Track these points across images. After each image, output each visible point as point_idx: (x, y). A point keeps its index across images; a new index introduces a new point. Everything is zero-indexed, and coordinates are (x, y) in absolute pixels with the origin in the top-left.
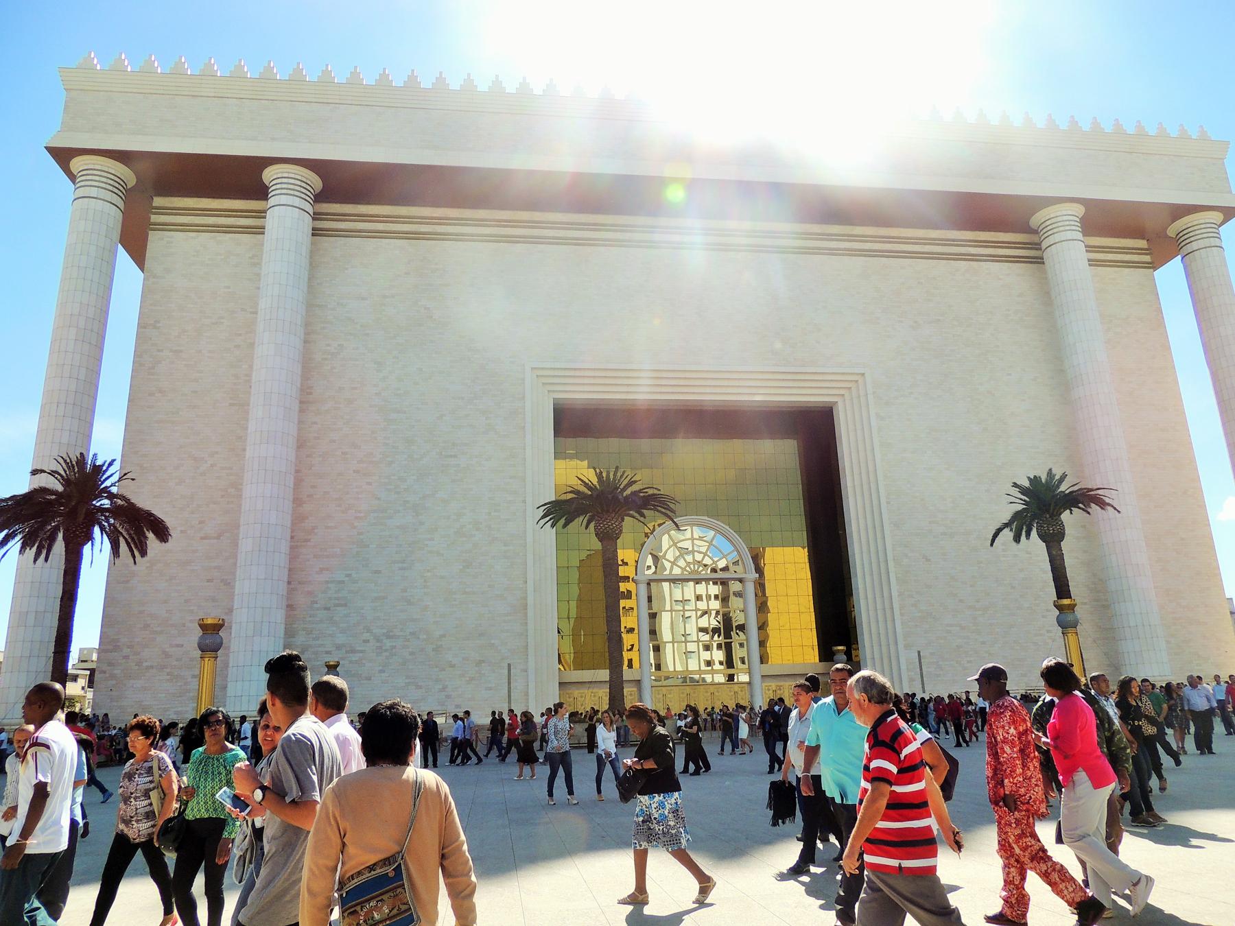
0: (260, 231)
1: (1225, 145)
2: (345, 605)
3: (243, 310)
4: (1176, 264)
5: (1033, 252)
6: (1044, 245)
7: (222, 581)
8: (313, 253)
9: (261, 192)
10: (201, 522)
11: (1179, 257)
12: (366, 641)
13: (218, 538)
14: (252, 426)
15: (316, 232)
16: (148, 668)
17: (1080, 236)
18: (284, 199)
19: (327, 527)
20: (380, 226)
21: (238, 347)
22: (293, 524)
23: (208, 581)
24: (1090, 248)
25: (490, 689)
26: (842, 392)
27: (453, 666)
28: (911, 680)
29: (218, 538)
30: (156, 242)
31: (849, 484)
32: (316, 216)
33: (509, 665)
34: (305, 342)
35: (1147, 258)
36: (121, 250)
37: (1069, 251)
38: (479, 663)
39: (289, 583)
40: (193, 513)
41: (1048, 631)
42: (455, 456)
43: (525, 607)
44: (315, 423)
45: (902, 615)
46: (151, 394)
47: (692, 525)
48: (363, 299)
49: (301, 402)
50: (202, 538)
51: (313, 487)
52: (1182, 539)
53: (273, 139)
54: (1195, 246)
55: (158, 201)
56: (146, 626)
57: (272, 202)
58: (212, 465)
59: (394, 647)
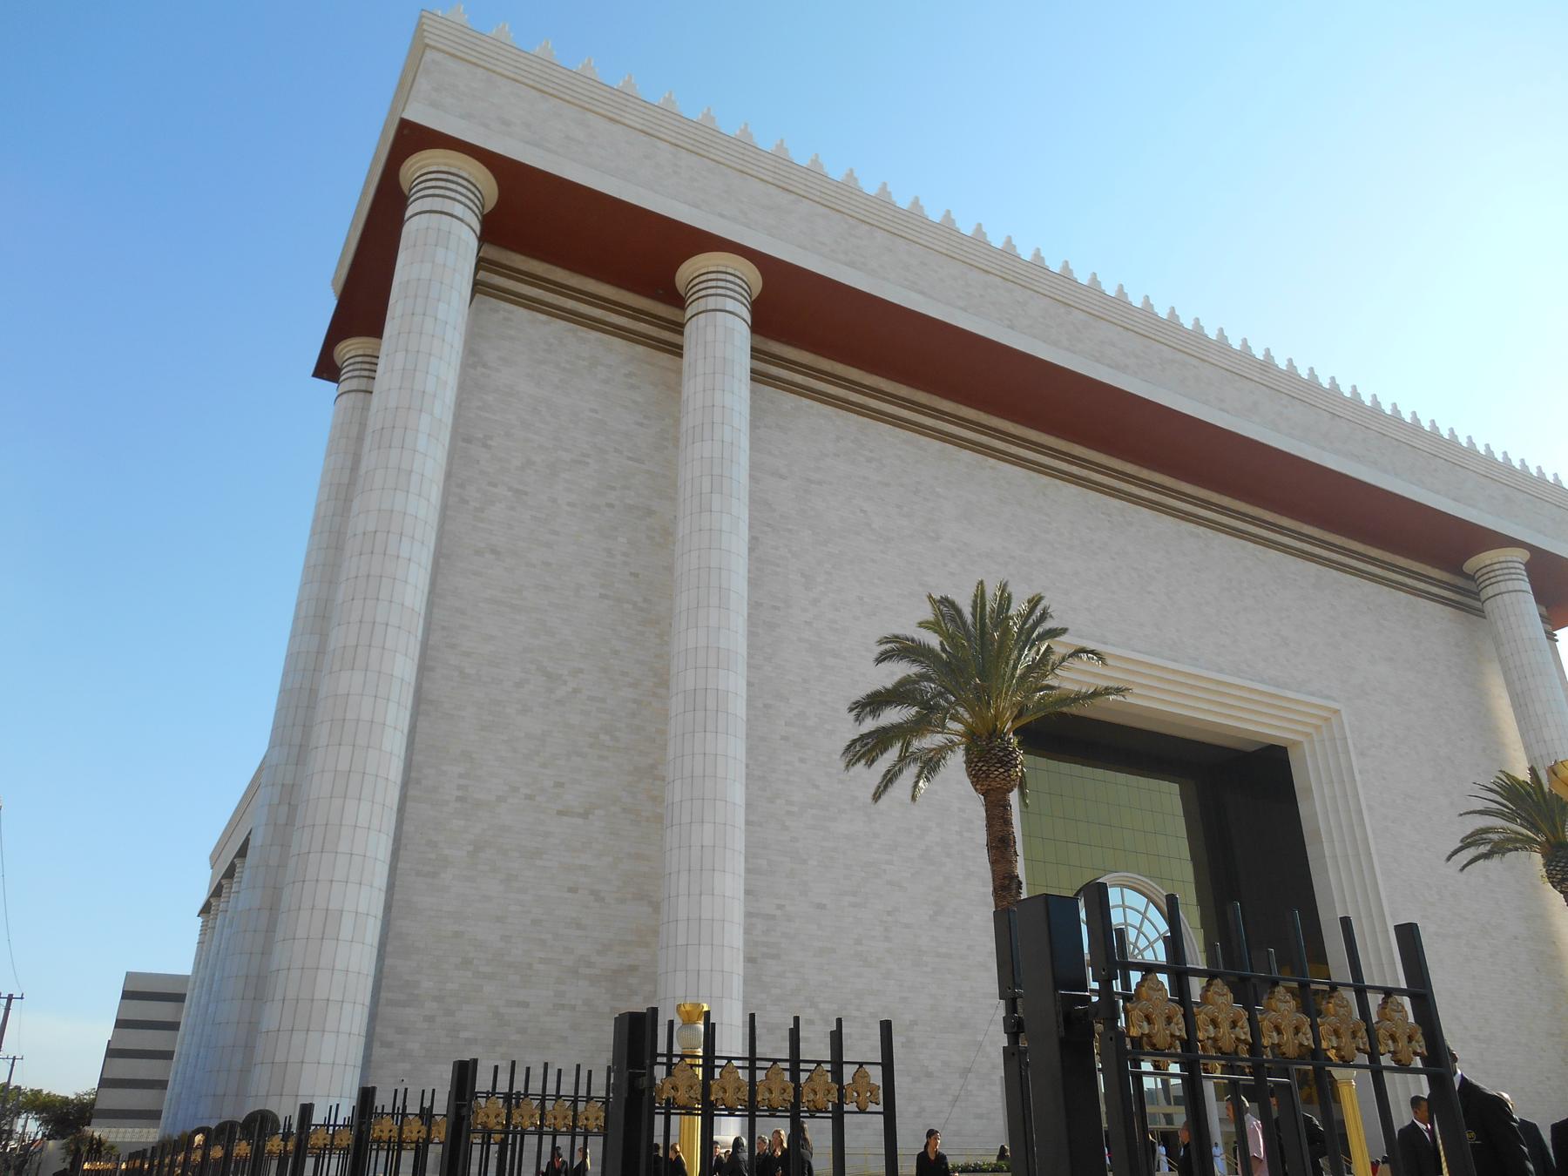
3: (616, 450)
5: (1468, 597)
10: (559, 785)
13: (585, 815)
20: (799, 378)
21: (610, 506)
23: (571, 890)
27: (929, 1075)
37: (1518, 603)
38: (965, 1072)
48: (782, 477)
50: (560, 813)
53: (722, 216)
58: (575, 691)
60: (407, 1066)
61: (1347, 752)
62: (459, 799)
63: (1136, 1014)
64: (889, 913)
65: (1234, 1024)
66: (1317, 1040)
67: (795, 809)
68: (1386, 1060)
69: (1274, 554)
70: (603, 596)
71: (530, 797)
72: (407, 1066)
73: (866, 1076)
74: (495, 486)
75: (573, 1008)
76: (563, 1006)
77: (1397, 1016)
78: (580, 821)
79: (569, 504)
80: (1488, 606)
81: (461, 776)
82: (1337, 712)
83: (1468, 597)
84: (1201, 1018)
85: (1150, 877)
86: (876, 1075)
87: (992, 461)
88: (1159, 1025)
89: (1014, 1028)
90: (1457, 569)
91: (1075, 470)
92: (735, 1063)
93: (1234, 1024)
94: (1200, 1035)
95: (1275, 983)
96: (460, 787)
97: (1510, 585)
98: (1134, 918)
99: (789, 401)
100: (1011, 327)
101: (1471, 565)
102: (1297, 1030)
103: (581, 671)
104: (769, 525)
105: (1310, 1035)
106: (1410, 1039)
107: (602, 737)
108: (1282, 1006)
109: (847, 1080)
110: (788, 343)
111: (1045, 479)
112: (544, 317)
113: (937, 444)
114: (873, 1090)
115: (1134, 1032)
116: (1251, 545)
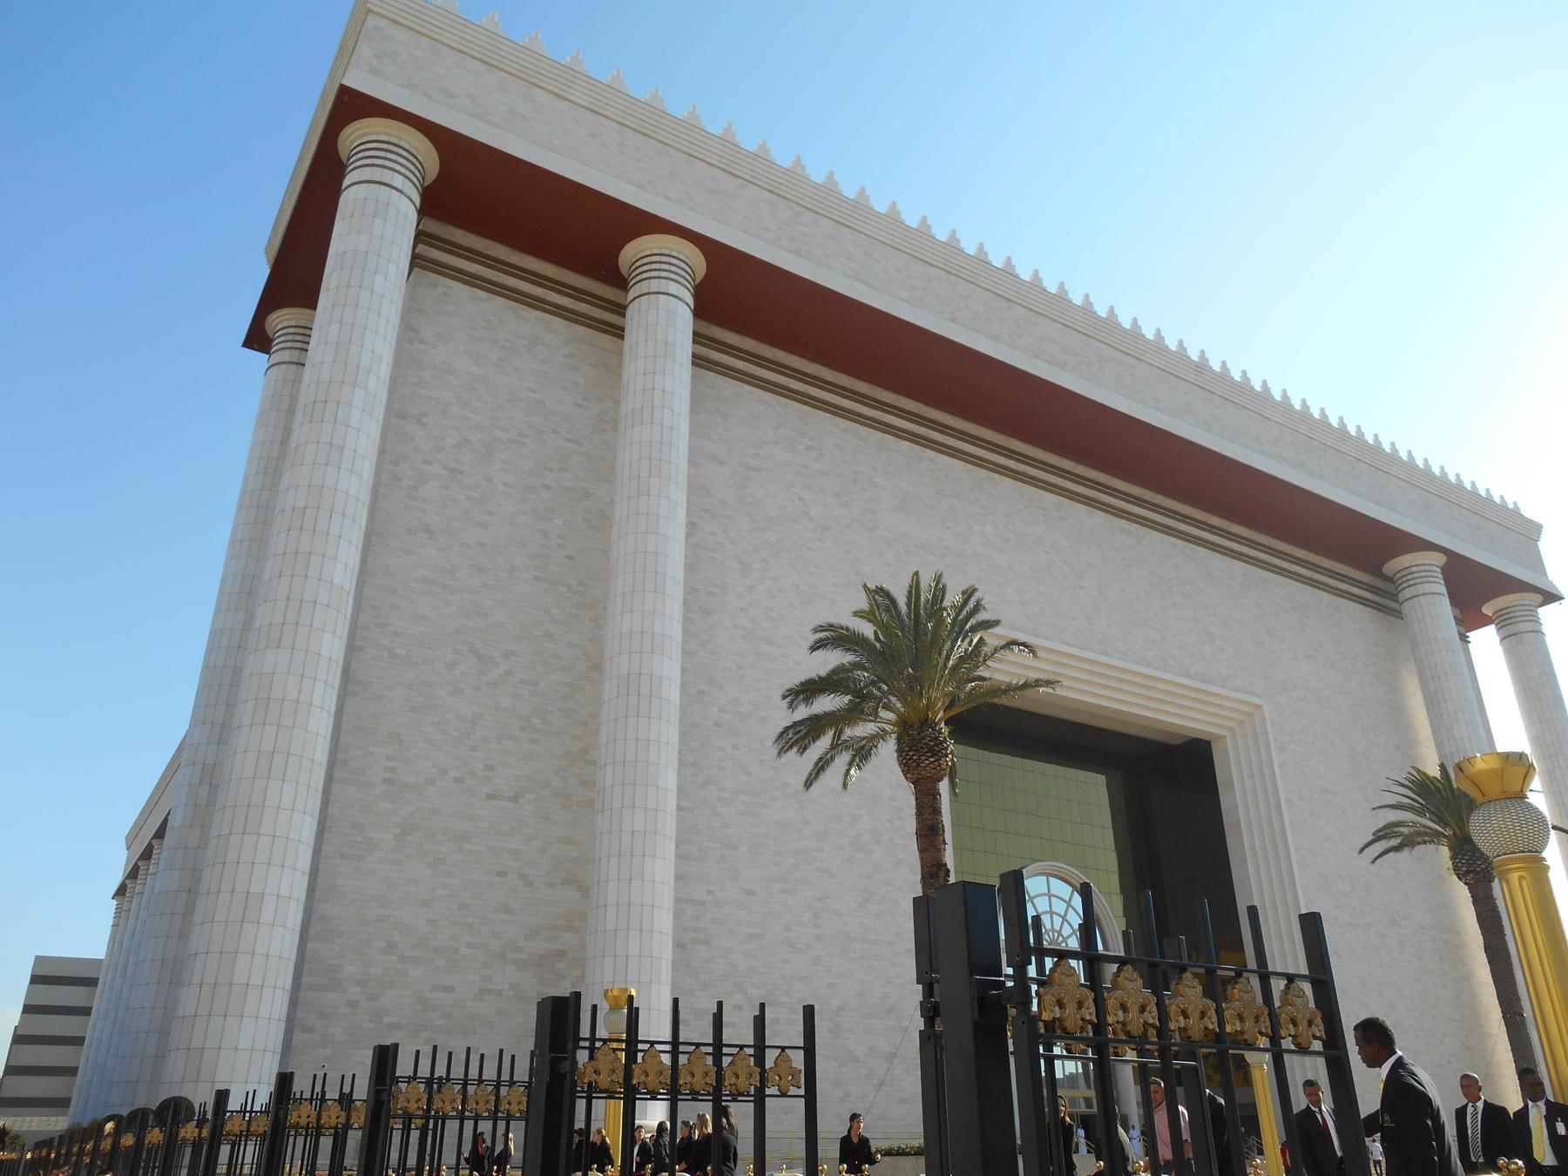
1: (1537, 528)
2: (706, 943)
3: (554, 431)
5: (1386, 598)
7: (522, 877)
13: (515, 799)
20: (740, 365)
23: (499, 874)
27: (855, 1060)
37: (1433, 605)
40: (474, 749)
46: (411, 532)
47: (1048, 875)
48: (721, 463)
50: (489, 797)
53: (666, 197)
56: (391, 947)
58: (507, 673)
60: (328, 1052)
61: (1269, 746)
62: (386, 781)
63: (1048, 999)
64: (818, 900)
65: (1143, 1009)
66: (1221, 1023)
67: (727, 795)
68: (1287, 1043)
69: (1202, 552)
70: (536, 578)
71: (457, 780)
72: (328, 1052)
73: (789, 1060)
74: (430, 464)
75: (500, 993)
76: (489, 991)
77: (1298, 1001)
78: (511, 805)
79: (505, 484)
80: (1406, 607)
81: (388, 758)
82: (1259, 707)
83: (1386, 598)
84: (1111, 1003)
85: (1076, 867)
86: (798, 1059)
87: (930, 453)
88: (1071, 1009)
89: (931, 1011)
90: (1376, 569)
92: (659, 1047)
93: (1143, 1009)
94: (1110, 1019)
95: (1183, 969)
96: (387, 769)
97: (1427, 588)
98: (1059, 907)
99: (730, 386)
100: (953, 320)
101: (1391, 567)
102: (1203, 1015)
103: (513, 653)
104: (707, 511)
105: (1215, 1019)
106: (1310, 1023)
107: (534, 720)
108: (1190, 992)
109: (769, 1064)
111: (983, 473)
113: (879, 435)
114: (795, 1073)
115: (1046, 1016)
116: (1181, 542)
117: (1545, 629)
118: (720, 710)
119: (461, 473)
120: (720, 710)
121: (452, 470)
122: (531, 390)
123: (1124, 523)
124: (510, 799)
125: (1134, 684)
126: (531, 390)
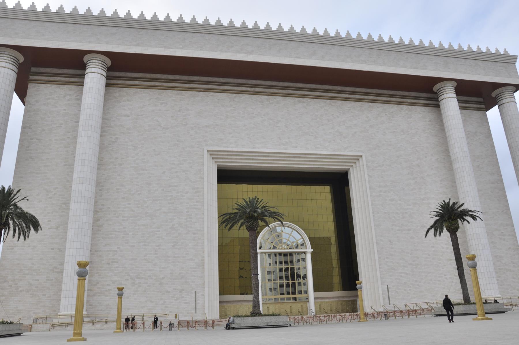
0: (82, 84)
3: (71, 120)
4: (496, 108)
6: (440, 99)
8: (106, 93)
9: (83, 67)
11: (497, 106)
12: (128, 280)
13: (57, 228)
14: (75, 176)
15: (108, 85)
16: (21, 291)
17: (455, 96)
18: (93, 70)
19: (109, 225)
20: (137, 83)
21: (68, 138)
22: (93, 223)
23: (52, 249)
24: (459, 101)
25: (186, 303)
26: (352, 164)
27: (169, 292)
28: (384, 299)
29: (57, 228)
30: (32, 89)
31: (355, 207)
32: (108, 78)
33: (196, 292)
34: (101, 136)
35: (483, 106)
36: (15, 93)
38: (181, 291)
39: (91, 251)
41: (445, 275)
42: (170, 192)
43: (203, 264)
44: (104, 175)
45: (380, 268)
46: (27, 160)
48: (128, 116)
49: (98, 165)
50: (49, 229)
51: (103, 205)
52: (502, 233)
54: (504, 101)
55: (33, 69)
57: (87, 71)
58: (55, 194)
59: (140, 283)
64: (157, 246)
74: (32, 139)
75: (52, 280)
79: (55, 140)
82: (361, 156)
91: (249, 89)
99: (132, 91)
101: (435, 89)
103: (57, 188)
110: (132, 72)
111: (235, 95)
112: (48, 85)
117: (516, 101)
118: (124, 194)
119: (42, 139)
120: (124, 194)
121: (39, 139)
122: (64, 110)
123: (301, 99)
124: (55, 229)
125: (300, 157)
126: (64, 110)
